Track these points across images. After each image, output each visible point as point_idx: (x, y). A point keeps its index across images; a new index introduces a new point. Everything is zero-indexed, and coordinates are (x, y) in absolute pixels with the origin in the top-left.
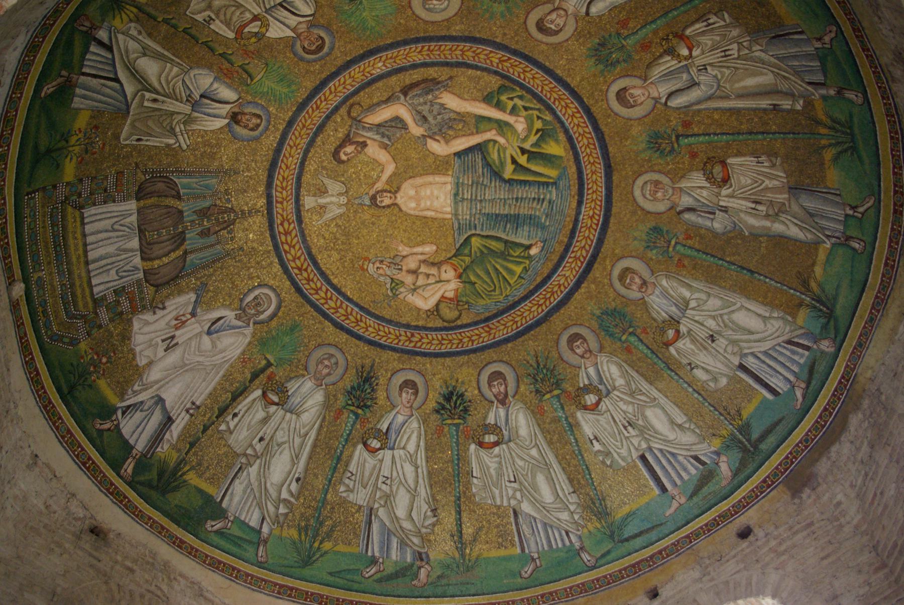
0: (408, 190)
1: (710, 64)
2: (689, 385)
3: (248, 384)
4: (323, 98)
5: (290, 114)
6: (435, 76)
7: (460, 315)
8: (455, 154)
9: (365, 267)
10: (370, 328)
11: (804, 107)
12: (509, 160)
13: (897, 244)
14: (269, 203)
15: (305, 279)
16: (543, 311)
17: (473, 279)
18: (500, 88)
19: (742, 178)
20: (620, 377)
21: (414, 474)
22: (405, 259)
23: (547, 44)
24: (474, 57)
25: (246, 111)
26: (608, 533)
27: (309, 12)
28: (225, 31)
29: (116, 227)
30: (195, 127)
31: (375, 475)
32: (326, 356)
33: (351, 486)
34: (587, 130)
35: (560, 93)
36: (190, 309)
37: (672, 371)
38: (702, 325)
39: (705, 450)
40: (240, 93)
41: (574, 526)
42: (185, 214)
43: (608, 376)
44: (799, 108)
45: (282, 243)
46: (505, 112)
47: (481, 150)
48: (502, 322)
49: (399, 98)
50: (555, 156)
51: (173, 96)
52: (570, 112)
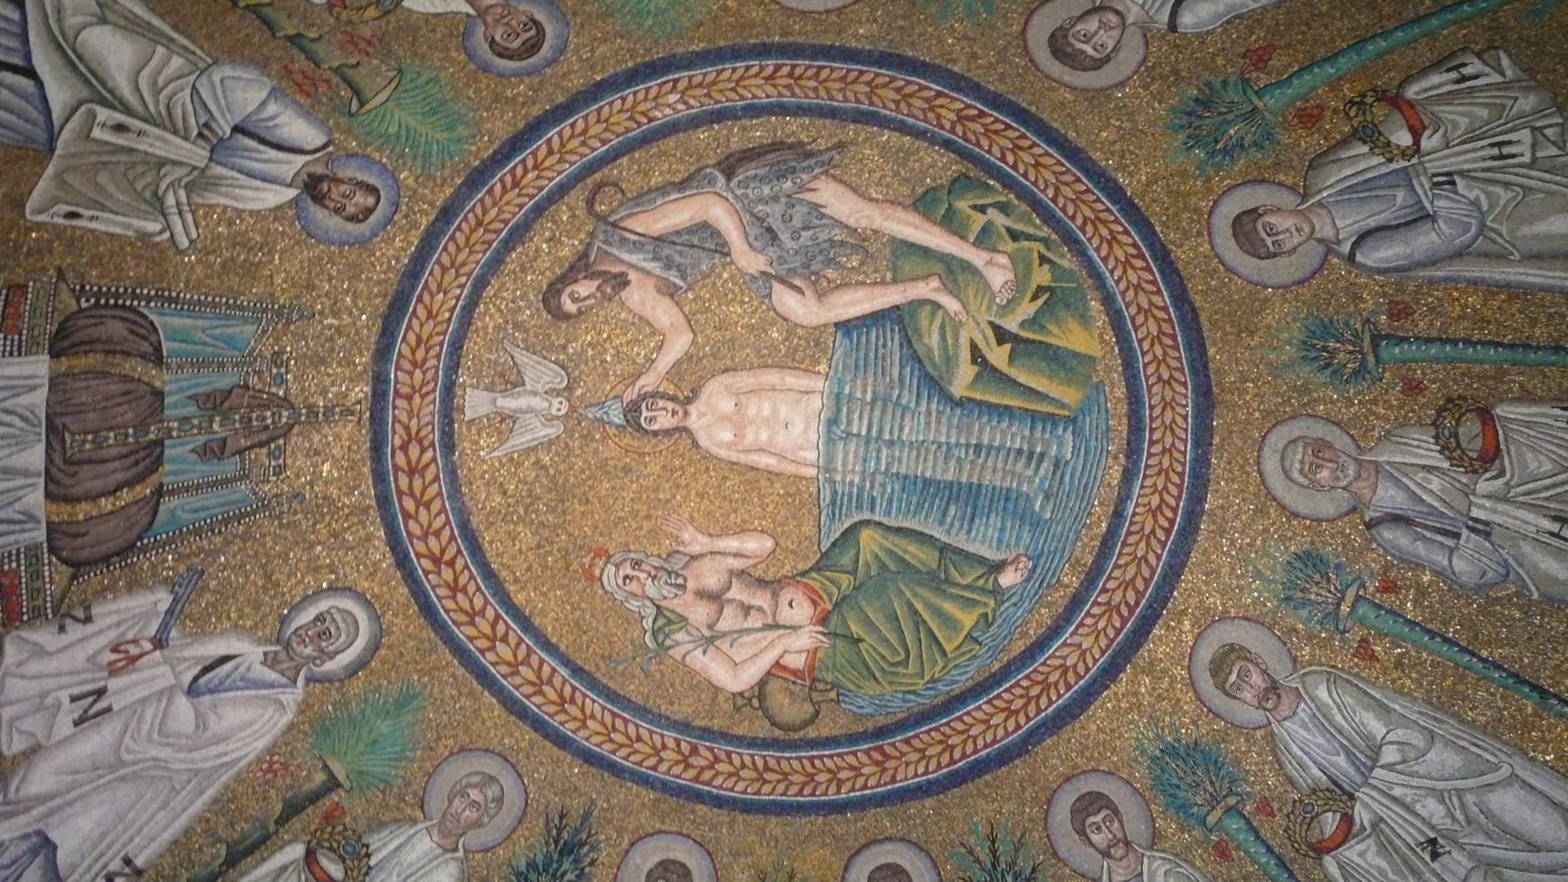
0: (717, 398)
1: (1461, 173)
3: (272, 828)
4: (530, 163)
5: (448, 191)
7: (817, 713)
8: (836, 325)
9: (597, 572)
12: (965, 354)
15: (448, 585)
16: (1018, 727)
17: (856, 629)
18: (956, 180)
19: (1529, 456)
24: (897, 103)
25: (341, 174)
30: (213, 199)
32: (476, 779)
34: (1157, 300)
35: (1099, 206)
36: (152, 630)
38: (1409, 809)
40: (330, 132)
42: (168, 400)
45: (400, 494)
46: (963, 238)
47: (900, 321)
48: (916, 743)
49: (712, 181)
50: (1076, 355)
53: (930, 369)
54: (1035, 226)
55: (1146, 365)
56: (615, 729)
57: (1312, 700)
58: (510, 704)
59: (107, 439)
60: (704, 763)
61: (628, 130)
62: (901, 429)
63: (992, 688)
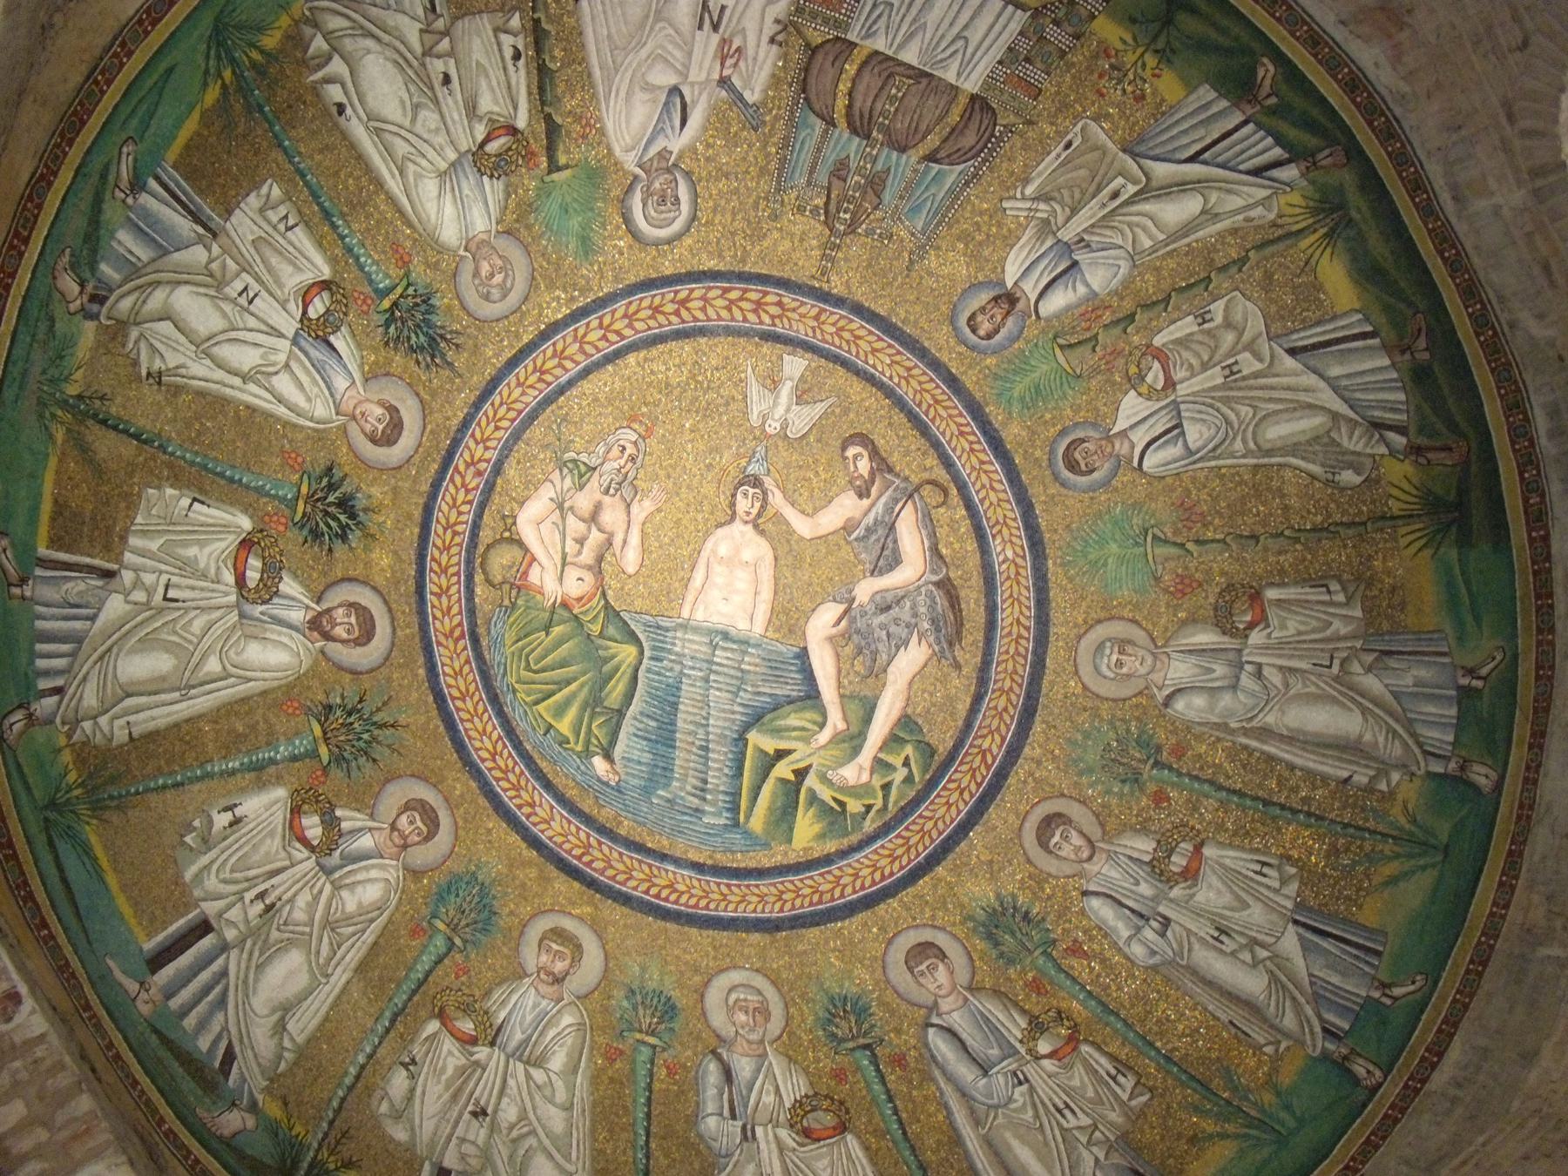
0: (756, 549)
1: (1032, 1090)
2: (370, 1057)
4: (976, 447)
6: (968, 639)
8: (805, 649)
9: (636, 426)
10: (519, 393)
12: (783, 745)
14: (824, 297)
16: (483, 760)
17: (557, 630)
18: (928, 744)
20: (360, 904)
21: (235, 364)
22: (622, 507)
23: (1020, 829)
24: (995, 708)
25: (1010, 321)
26: (61, 798)
27: (1146, 464)
28: (1171, 333)
29: (960, 43)
30: (1029, 233)
31: (266, 277)
33: (270, 213)
34: (849, 890)
35: (921, 848)
36: (736, 81)
37: (393, 1021)
38: (502, 1092)
39: (249, 1075)
40: (1048, 320)
41: (71, 714)
43: (360, 877)
47: (808, 697)
48: (466, 669)
49: (934, 572)
50: (791, 829)
51: (1105, 222)
52: (884, 862)
53: (769, 717)
54: (896, 802)
55: (792, 882)
56: (509, 409)
57: (559, 1012)
58: (555, 328)
59: (891, 104)
60: (468, 479)
61: (988, 519)
62: (718, 689)
63: (511, 741)
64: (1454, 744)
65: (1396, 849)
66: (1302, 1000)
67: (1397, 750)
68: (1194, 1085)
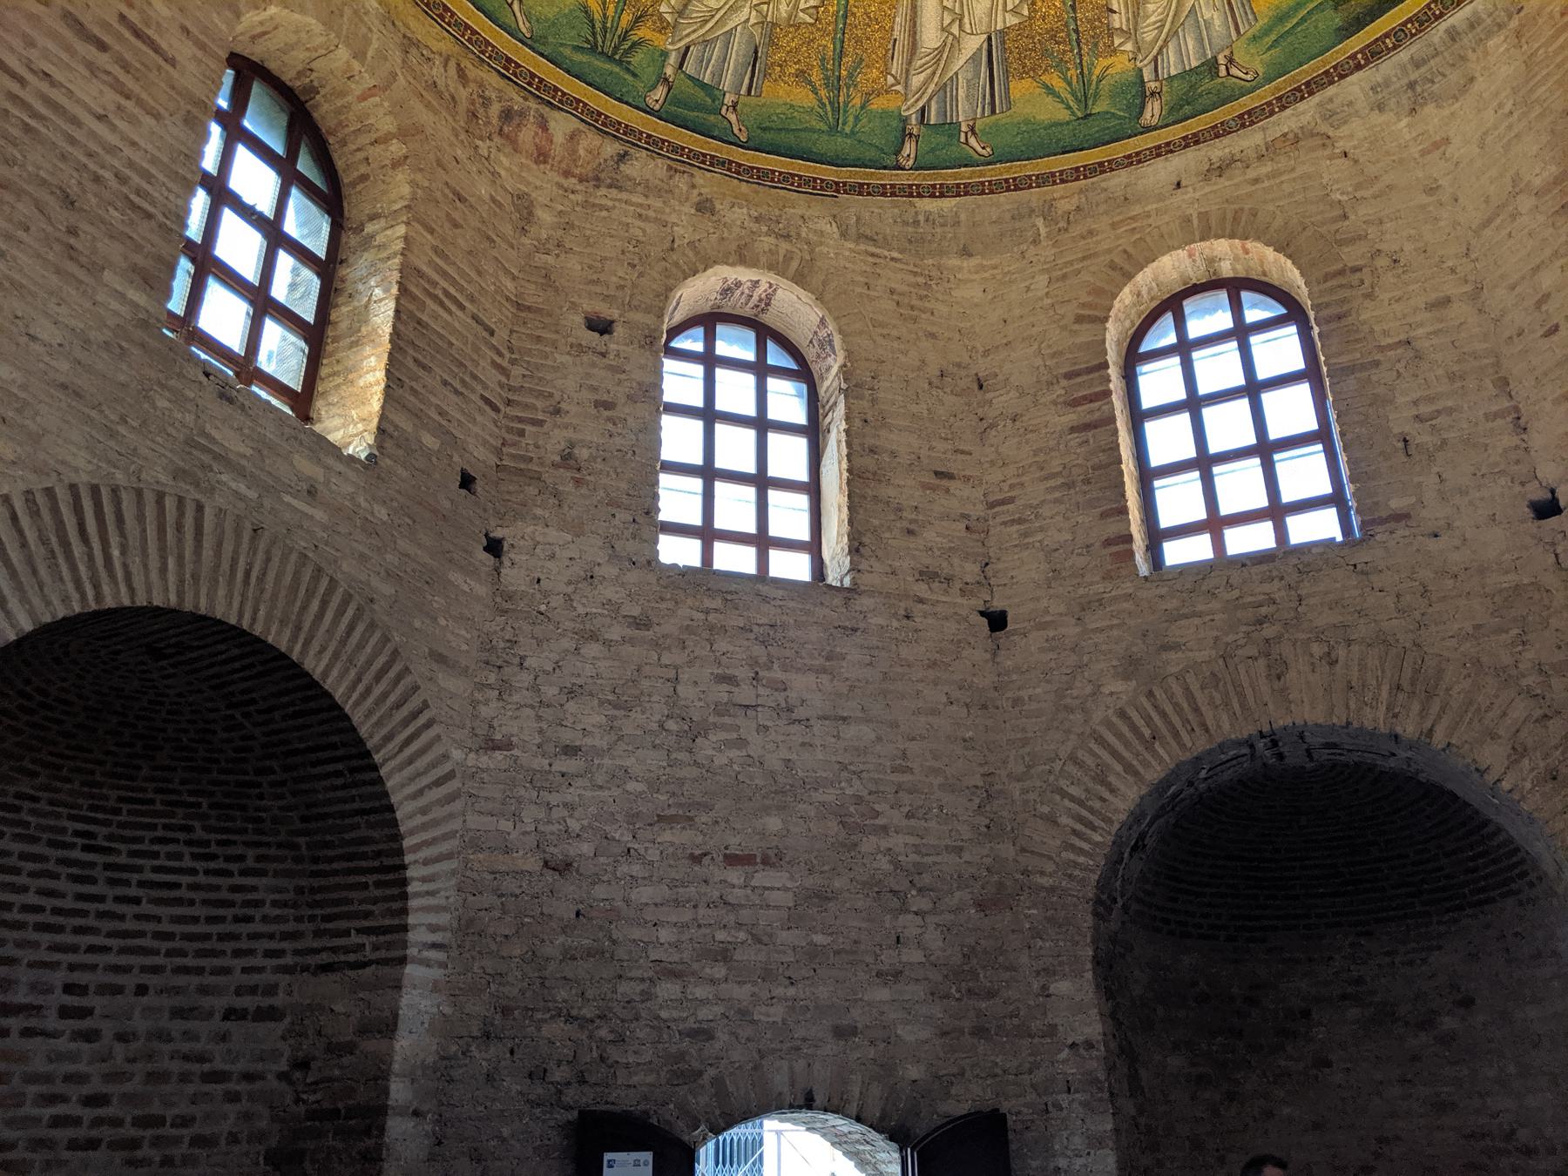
11: (661, 18)
13: (469, 40)
44: (663, 8)
64: (1171, 79)
65: (1074, 80)
66: (936, 79)
67: (1149, 37)
68: (838, 46)
